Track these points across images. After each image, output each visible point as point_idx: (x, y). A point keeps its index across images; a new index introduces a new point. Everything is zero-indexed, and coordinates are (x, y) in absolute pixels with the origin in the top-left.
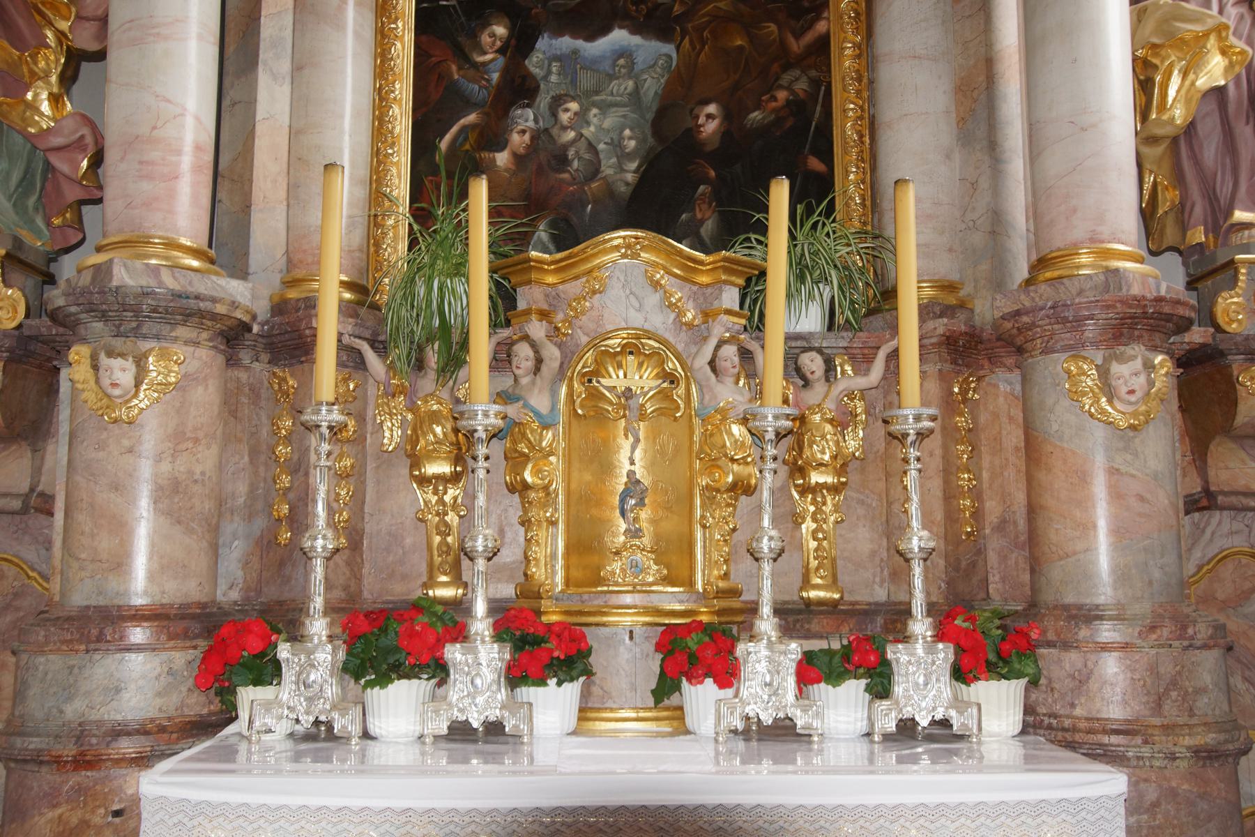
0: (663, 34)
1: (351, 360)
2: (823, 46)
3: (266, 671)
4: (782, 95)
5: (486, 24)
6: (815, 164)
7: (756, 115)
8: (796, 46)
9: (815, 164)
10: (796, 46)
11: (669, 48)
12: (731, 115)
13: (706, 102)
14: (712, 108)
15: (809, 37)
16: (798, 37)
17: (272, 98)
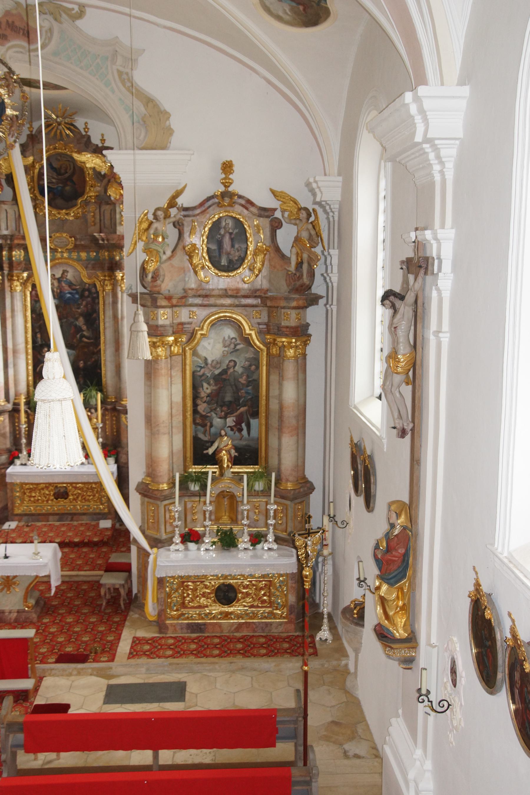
0: (73, 349)
1: (26, 412)
2: (100, 350)
3: (18, 458)
4: (93, 359)
5: (44, 348)
6: (99, 371)
7: (89, 363)
8: (95, 351)
9: (99, 371)
10: (95, 351)
11: (74, 352)
12: (85, 363)
13: (80, 361)
14: (82, 362)
15: (98, 349)
16: (96, 349)
17: (11, 371)
